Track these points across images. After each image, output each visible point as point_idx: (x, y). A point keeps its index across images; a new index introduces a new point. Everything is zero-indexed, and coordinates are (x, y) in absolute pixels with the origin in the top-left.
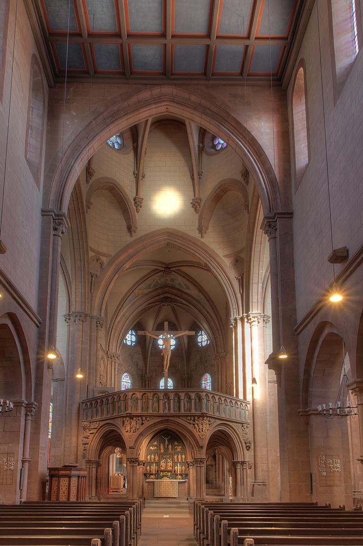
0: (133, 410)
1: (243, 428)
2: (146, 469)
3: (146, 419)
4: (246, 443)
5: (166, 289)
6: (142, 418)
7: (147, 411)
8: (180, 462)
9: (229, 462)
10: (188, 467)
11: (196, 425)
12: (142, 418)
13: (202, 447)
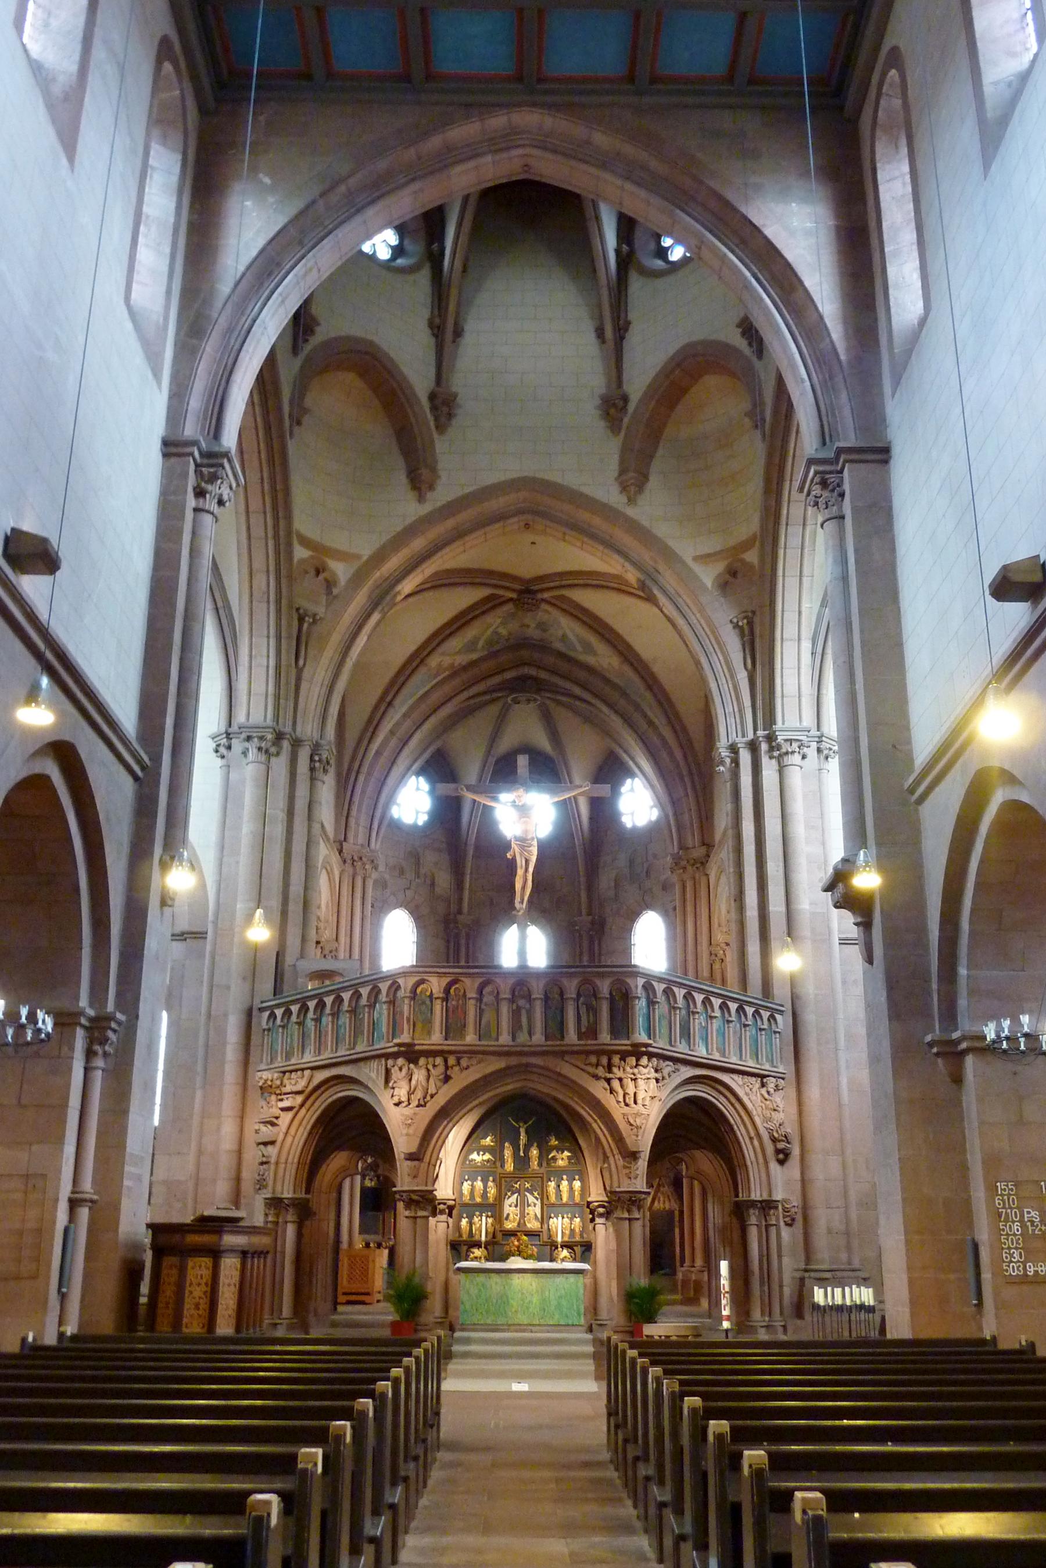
0: (417, 1035)
3: (459, 1063)
5: (525, 653)
6: (446, 1061)
9: (722, 1204)
10: (592, 1220)
11: (616, 1084)
12: (446, 1061)
13: (634, 1156)
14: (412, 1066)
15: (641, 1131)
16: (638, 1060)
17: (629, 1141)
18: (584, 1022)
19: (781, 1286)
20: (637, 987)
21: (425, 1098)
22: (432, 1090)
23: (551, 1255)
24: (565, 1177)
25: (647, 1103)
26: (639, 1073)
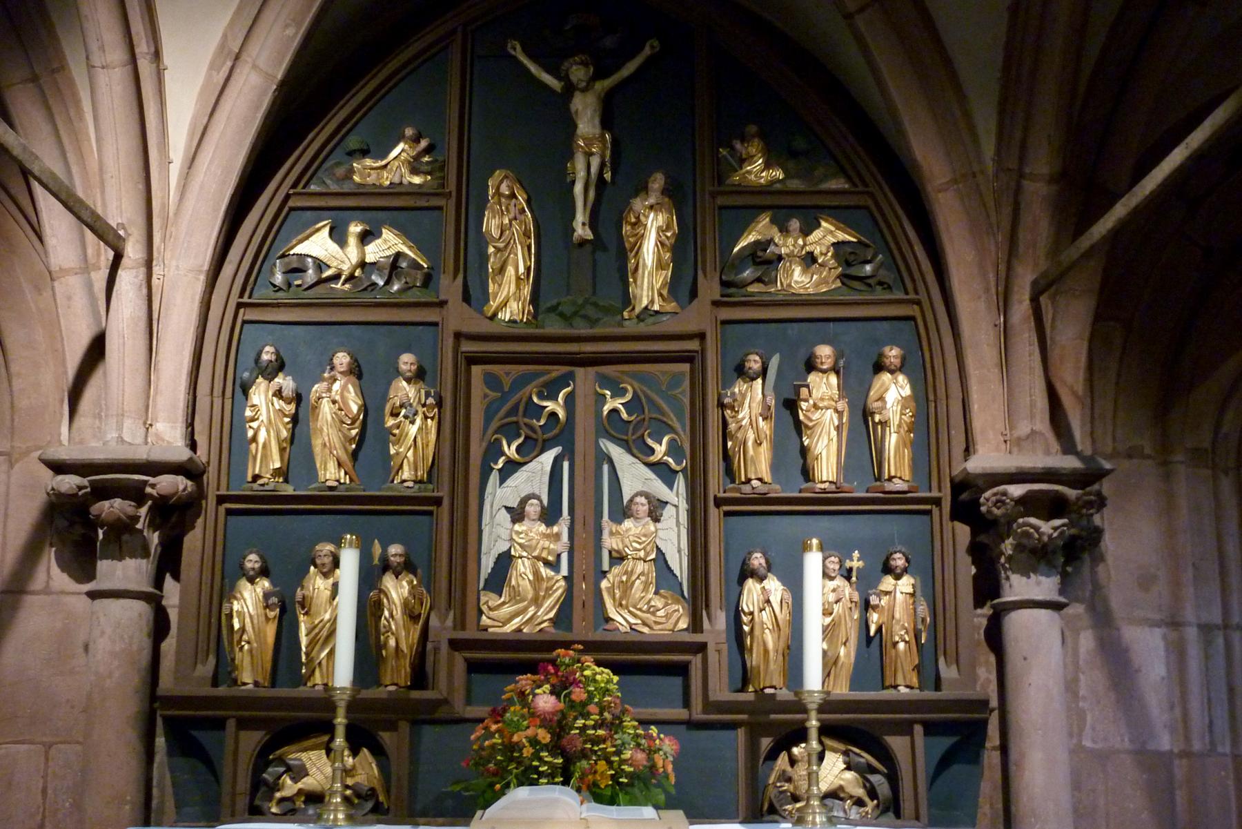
23: (755, 784)
24: (824, 352)
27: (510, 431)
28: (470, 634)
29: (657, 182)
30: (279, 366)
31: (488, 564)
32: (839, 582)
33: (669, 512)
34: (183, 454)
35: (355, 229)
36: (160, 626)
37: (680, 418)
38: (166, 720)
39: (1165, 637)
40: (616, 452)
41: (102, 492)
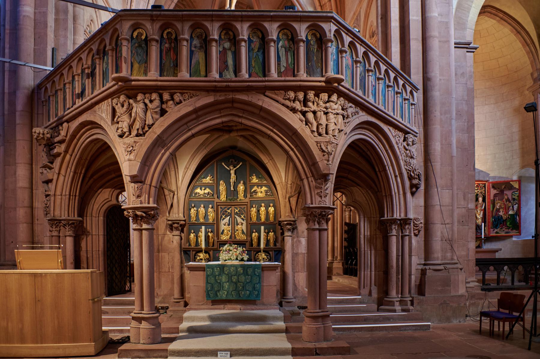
0: (135, 72)
1: (405, 144)
2: (188, 240)
3: (172, 99)
4: (411, 178)
7: (175, 75)
8: (263, 224)
10: (282, 234)
11: (310, 116)
13: (325, 177)
14: (131, 101)
15: (331, 157)
16: (329, 97)
17: (322, 164)
18: (283, 63)
19: (410, 275)
20: (330, 31)
21: (143, 128)
22: (149, 121)
24: (263, 204)
25: (336, 134)
26: (330, 107)
27: (223, 214)
28: (219, 240)
29: (242, 182)
30: (195, 206)
31: (221, 231)
32: (264, 233)
33: (243, 224)
34: (184, 219)
35: (203, 188)
36: (181, 239)
37: (245, 212)
38: (183, 250)
39: (305, 239)
40: (236, 216)
41: (174, 223)
